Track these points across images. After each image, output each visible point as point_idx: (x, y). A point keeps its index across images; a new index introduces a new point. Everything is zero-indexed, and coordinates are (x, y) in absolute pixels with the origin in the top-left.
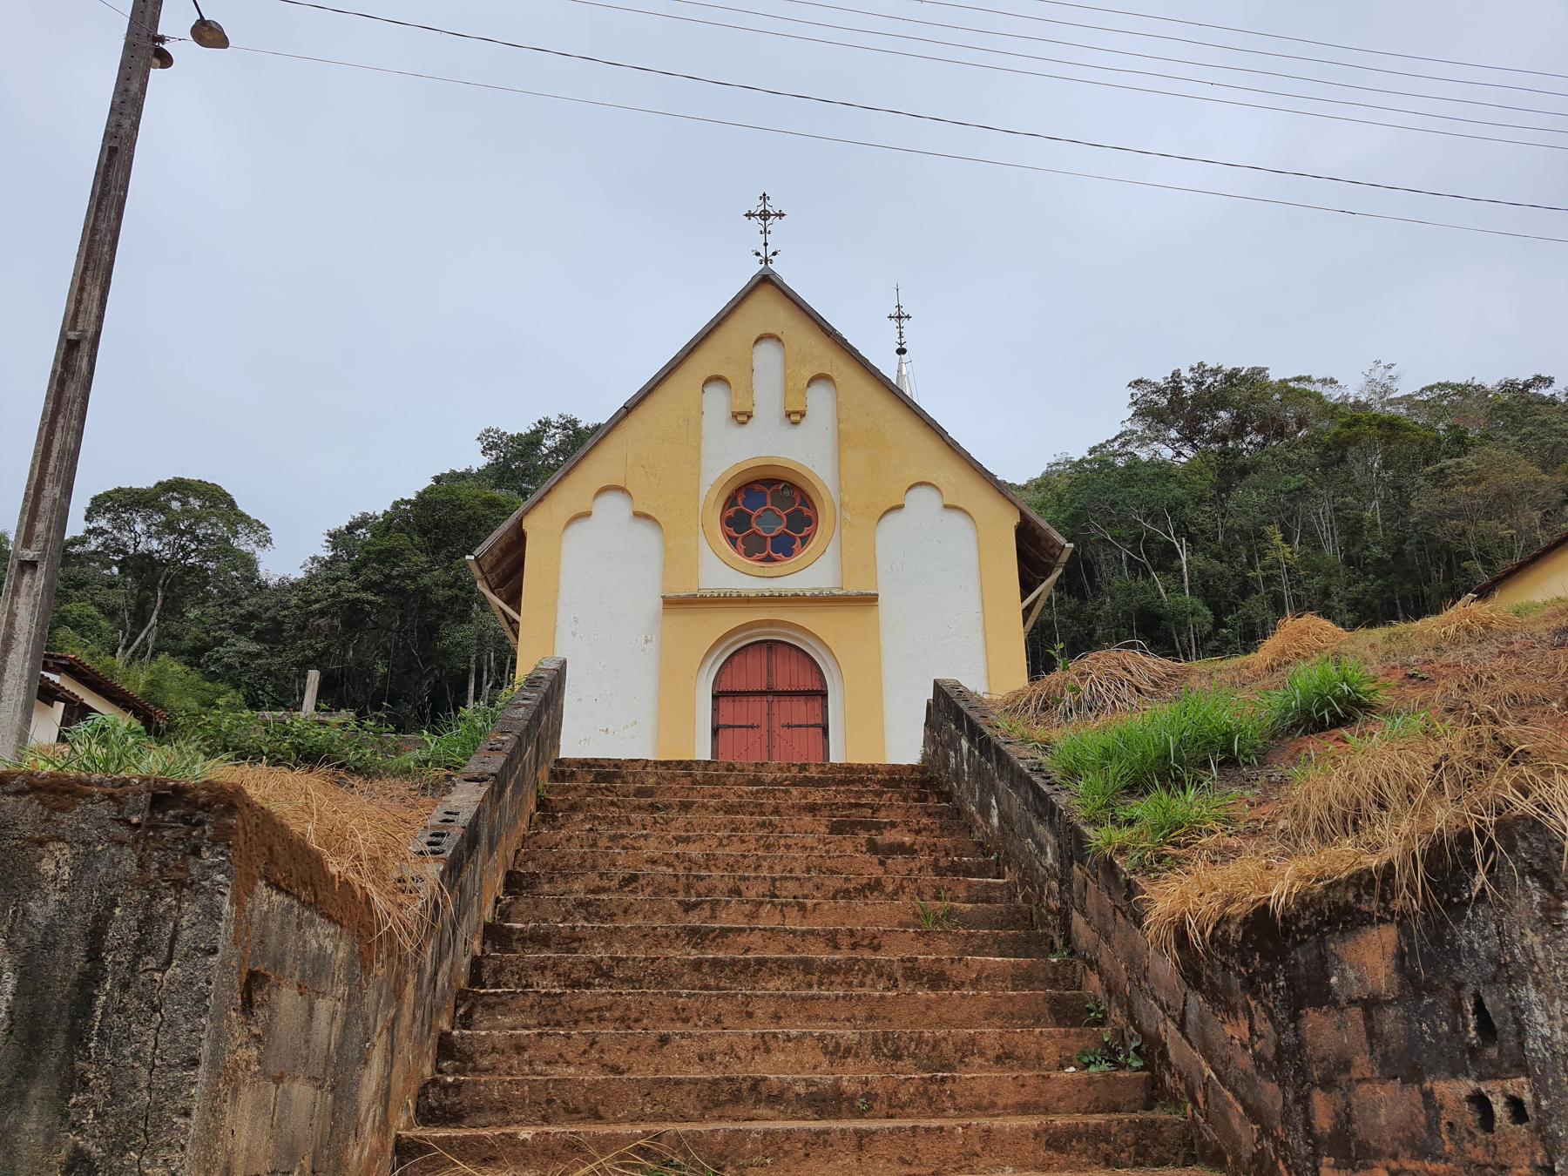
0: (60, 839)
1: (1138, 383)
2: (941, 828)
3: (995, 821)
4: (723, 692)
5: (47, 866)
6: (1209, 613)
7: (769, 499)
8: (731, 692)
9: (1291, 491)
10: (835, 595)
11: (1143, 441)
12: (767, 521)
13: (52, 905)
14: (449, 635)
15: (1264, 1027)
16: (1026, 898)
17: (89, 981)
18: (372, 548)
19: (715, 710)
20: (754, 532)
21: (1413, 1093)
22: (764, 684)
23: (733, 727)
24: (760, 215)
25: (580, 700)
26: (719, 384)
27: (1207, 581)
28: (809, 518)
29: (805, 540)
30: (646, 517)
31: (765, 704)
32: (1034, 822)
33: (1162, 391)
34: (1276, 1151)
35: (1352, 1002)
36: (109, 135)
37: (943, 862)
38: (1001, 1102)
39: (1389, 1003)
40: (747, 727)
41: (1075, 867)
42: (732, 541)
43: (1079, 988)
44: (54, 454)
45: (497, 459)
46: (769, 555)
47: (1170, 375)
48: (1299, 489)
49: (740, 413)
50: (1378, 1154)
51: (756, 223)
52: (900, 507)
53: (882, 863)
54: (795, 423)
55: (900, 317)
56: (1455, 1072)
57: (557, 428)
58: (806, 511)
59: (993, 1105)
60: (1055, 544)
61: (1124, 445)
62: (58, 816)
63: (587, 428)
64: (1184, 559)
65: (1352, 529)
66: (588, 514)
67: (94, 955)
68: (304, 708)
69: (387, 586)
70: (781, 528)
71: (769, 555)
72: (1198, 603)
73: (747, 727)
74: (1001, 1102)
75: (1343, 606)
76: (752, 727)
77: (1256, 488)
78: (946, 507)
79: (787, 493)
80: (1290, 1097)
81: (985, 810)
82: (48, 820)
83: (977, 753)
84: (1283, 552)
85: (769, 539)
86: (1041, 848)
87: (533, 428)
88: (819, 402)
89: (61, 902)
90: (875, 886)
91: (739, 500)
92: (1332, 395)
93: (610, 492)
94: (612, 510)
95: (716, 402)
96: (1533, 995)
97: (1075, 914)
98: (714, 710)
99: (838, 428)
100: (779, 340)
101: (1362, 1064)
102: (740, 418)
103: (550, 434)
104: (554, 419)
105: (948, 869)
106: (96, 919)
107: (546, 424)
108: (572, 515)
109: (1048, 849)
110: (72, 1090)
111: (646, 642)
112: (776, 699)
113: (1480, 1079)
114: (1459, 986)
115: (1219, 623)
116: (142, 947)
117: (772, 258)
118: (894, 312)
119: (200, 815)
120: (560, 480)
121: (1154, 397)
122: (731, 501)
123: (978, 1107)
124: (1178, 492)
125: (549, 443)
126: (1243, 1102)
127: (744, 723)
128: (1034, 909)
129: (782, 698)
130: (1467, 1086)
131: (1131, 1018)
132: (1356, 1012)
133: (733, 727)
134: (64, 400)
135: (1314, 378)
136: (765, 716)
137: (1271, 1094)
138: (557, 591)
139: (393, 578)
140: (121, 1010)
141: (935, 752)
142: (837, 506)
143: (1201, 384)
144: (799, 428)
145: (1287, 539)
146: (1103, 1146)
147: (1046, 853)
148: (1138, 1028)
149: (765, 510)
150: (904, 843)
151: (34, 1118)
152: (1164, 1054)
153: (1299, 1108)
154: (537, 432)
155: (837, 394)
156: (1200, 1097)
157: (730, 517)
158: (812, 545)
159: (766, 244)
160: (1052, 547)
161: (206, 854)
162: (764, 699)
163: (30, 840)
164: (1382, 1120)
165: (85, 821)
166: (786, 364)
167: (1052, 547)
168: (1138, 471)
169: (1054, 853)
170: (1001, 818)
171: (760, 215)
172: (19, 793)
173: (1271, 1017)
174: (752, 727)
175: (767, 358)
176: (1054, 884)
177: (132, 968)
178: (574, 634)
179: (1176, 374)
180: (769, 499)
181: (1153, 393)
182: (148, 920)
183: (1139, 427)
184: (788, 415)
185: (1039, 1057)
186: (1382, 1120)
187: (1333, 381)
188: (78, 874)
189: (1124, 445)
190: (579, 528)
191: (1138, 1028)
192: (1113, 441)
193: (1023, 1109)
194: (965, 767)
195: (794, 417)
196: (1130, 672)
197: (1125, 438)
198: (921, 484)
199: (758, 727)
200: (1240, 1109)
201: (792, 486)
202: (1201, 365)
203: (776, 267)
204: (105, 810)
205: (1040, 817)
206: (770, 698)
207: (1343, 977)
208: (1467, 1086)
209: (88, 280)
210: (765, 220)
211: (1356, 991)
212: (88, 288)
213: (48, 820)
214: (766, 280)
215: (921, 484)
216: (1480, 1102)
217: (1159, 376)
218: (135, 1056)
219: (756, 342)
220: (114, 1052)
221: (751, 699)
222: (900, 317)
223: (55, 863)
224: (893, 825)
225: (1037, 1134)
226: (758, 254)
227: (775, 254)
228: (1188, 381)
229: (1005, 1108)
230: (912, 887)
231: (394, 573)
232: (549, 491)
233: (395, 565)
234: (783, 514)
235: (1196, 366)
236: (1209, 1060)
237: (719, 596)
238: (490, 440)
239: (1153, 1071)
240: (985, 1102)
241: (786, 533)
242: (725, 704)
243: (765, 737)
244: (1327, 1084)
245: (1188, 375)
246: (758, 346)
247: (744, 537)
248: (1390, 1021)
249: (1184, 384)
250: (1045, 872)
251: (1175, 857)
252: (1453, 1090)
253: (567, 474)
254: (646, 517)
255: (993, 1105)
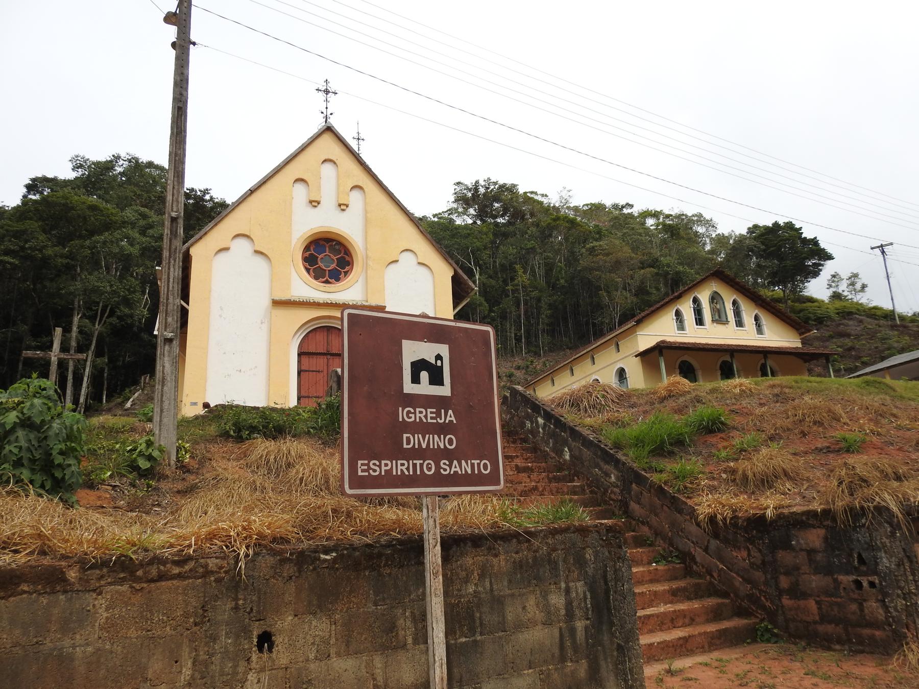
0: (589, 547)
1: (458, 183)
2: (535, 457)
3: (567, 457)
4: (304, 352)
5: (587, 556)
6: (487, 305)
7: (327, 249)
8: (308, 353)
9: (527, 249)
10: (364, 305)
11: (459, 214)
12: (328, 262)
13: (592, 569)
14: (65, 287)
15: (757, 554)
16: (591, 492)
17: (607, 592)
18: (11, 228)
19: (299, 362)
20: (319, 267)
21: (829, 579)
22: (325, 349)
23: (309, 371)
24: (324, 91)
25: (225, 353)
26: (302, 183)
27: (486, 289)
28: (348, 261)
29: (346, 273)
30: (261, 253)
31: (326, 360)
32: (602, 464)
33: (470, 190)
34: (760, 594)
35: (802, 550)
36: (175, 100)
37: (551, 475)
38: (645, 579)
39: (819, 552)
40: (316, 371)
41: (634, 485)
42: (308, 270)
43: (633, 531)
44: (171, 280)
45: (83, 175)
46: (327, 280)
47: (474, 182)
48: (531, 248)
49: (314, 201)
50: (810, 595)
51: (322, 95)
52: (397, 261)
53: (529, 477)
54: (343, 210)
55: (358, 139)
56: (848, 573)
57: (125, 161)
58: (347, 258)
59: (643, 581)
60: (469, 287)
61: (449, 214)
62: (586, 539)
63: (142, 162)
64: (477, 277)
65: (549, 268)
66: (227, 249)
67: (606, 583)
68: (53, 350)
69: (21, 254)
70: (333, 266)
71: (327, 280)
72: (482, 300)
73: (316, 371)
74: (645, 579)
75: (546, 306)
76: (319, 372)
77: (512, 245)
78: (419, 263)
79: (337, 247)
80: (769, 576)
81: (560, 453)
82: (584, 541)
83: (552, 426)
84: (523, 278)
85: (327, 271)
86: (608, 475)
87: (109, 159)
88: (355, 199)
89: (594, 568)
90: (535, 488)
91: (312, 248)
92: (545, 201)
93: (241, 237)
94: (241, 248)
95: (300, 193)
96: (883, 555)
97: (632, 503)
98: (298, 362)
99: (366, 215)
100: (335, 163)
101: (805, 568)
102: (314, 204)
103: (120, 163)
104: (123, 155)
105: (553, 478)
106: (604, 572)
107: (117, 158)
108: (219, 249)
109: (612, 476)
110: (612, 626)
111: (262, 323)
112: (332, 357)
113: (858, 576)
114: (852, 550)
115: (491, 311)
116: (617, 580)
117: (330, 116)
118: (356, 136)
119: (618, 535)
120: (212, 228)
121: (465, 191)
122: (307, 248)
123: (639, 582)
124: (478, 244)
125: (119, 169)
126: (742, 577)
127: (315, 369)
128: (599, 497)
129: (334, 357)
130: (852, 578)
131: (671, 544)
132: (804, 553)
133: (309, 371)
134: (173, 250)
135: (539, 193)
136: (325, 367)
137: (758, 575)
138: (210, 291)
139: (26, 249)
140: (617, 600)
141: (512, 418)
142: (365, 257)
143: (488, 188)
144: (345, 213)
145: (525, 272)
146: (686, 593)
147: (610, 477)
148: (677, 549)
149: (326, 255)
150: (529, 466)
151: (606, 635)
152: (693, 559)
153: (773, 581)
154: (111, 161)
155: (365, 198)
156: (715, 575)
157: (306, 257)
158: (351, 276)
159: (327, 108)
160: (467, 288)
161: (623, 548)
162: (325, 357)
163: (581, 548)
164: (814, 586)
165: (592, 540)
166: (338, 178)
167: (467, 288)
168: (460, 231)
169: (617, 478)
170: (571, 456)
171: (324, 91)
172: (574, 532)
173: (760, 551)
174: (319, 372)
175: (328, 170)
176: (617, 490)
177: (616, 587)
178: (220, 316)
179: (477, 182)
180: (327, 249)
181: (465, 189)
182: (616, 571)
183: (455, 205)
184: (340, 205)
185: (642, 561)
186: (814, 586)
187: (546, 196)
188: (595, 559)
189: (449, 214)
190: (222, 255)
191: (677, 549)
192: (445, 212)
193: (652, 581)
194: (541, 430)
195: (343, 207)
196: (607, 392)
197: (451, 211)
198: (407, 250)
199: (322, 372)
200: (741, 580)
201: (339, 243)
202: (489, 179)
203: (334, 122)
204: (595, 535)
205: (607, 463)
206: (329, 357)
207: (798, 541)
208: (852, 578)
209: (176, 183)
210: (327, 94)
211: (804, 546)
212: (176, 187)
213: (584, 541)
214: (329, 129)
215: (407, 250)
216: (858, 584)
217: (469, 182)
218: (624, 613)
219: (323, 162)
220: (619, 613)
221: (318, 357)
222: (358, 139)
223: (589, 555)
224: (517, 457)
225: (669, 591)
226: (322, 113)
227: (331, 114)
228: (483, 187)
229: (646, 581)
230: (548, 488)
231: (27, 246)
232: (206, 234)
233: (26, 241)
234: (335, 258)
235: (486, 179)
236: (722, 562)
237: (303, 301)
238: (78, 162)
239: (685, 564)
240: (640, 580)
241: (336, 269)
242: (304, 358)
243: (326, 378)
244: (787, 574)
245: (483, 183)
246: (323, 165)
247: (314, 269)
248: (819, 557)
249: (480, 187)
250: (608, 484)
251: (691, 488)
252: (846, 579)
253: (216, 225)
254: (261, 253)
255: (643, 581)
